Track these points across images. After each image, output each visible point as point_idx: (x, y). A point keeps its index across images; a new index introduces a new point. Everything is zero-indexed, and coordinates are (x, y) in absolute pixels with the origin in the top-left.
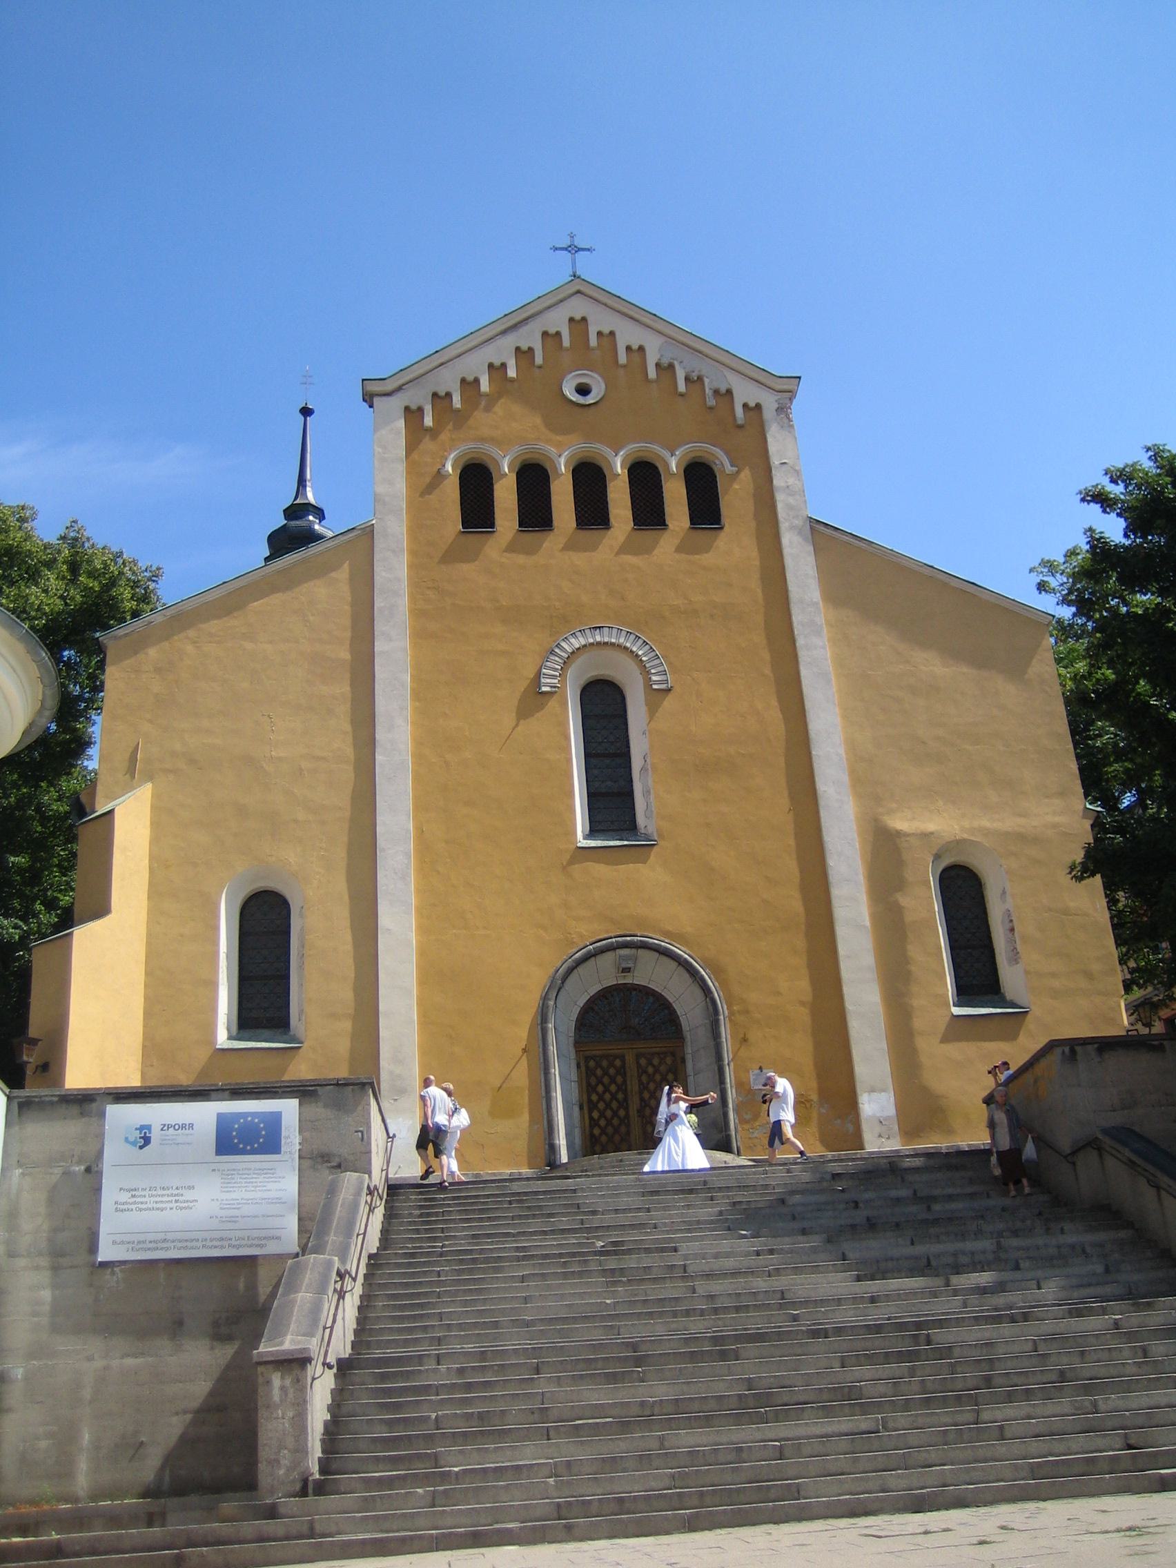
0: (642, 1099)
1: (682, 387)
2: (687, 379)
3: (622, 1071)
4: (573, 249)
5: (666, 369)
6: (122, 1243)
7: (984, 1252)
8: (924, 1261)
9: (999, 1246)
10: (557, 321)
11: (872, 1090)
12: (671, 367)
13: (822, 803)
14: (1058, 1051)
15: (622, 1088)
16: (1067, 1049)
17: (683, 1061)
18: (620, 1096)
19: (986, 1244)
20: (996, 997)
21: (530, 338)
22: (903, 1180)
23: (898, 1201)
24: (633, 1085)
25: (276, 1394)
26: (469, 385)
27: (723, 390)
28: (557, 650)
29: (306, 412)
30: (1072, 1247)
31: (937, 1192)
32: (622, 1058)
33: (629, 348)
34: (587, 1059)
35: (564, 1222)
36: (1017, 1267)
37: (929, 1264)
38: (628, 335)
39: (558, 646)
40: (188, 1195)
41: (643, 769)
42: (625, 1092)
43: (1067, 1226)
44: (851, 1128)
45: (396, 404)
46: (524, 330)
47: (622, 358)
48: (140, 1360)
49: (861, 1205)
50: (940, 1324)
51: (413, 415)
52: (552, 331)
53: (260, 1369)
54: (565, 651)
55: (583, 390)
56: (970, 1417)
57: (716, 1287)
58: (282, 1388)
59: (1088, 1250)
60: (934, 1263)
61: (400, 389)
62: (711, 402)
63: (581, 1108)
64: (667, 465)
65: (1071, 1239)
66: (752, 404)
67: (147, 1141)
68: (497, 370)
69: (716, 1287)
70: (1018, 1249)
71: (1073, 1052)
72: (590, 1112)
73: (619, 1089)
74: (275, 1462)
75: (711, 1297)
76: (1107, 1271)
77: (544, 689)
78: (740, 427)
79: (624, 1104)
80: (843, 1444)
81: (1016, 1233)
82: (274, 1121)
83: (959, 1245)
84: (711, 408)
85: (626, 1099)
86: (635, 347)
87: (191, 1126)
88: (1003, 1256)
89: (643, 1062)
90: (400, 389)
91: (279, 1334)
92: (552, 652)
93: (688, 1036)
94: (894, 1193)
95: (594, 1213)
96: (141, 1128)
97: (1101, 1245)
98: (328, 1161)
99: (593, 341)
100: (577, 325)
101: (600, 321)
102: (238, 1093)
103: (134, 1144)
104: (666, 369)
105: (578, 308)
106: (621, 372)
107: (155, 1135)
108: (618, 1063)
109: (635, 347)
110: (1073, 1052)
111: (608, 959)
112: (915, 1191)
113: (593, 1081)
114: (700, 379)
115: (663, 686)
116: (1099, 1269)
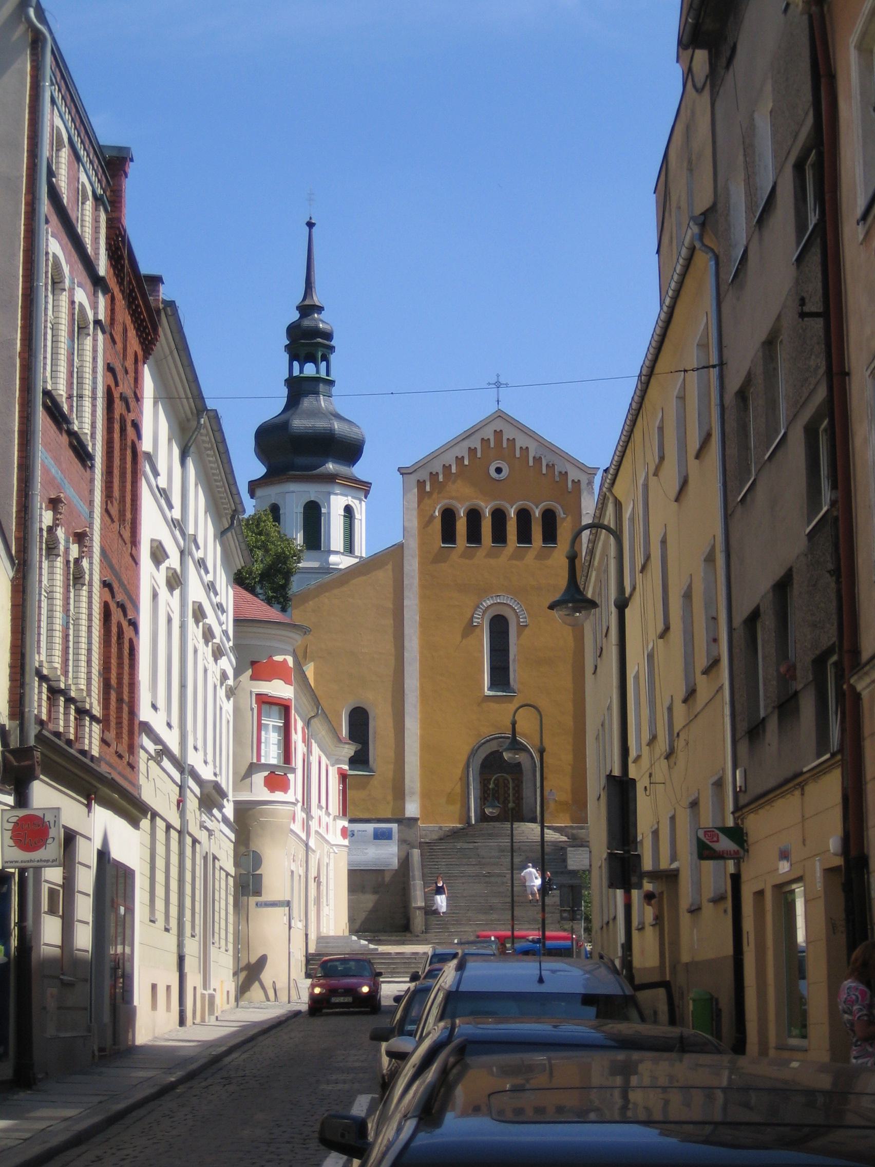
1: (544, 471)
2: (547, 465)
4: (498, 385)
5: (538, 460)
10: (488, 433)
12: (540, 458)
17: (522, 782)
21: (475, 443)
26: (447, 468)
29: (310, 225)
34: (484, 780)
38: (522, 441)
39: (482, 604)
40: (366, 851)
41: (514, 660)
45: (413, 479)
46: (473, 437)
47: (518, 455)
51: (421, 484)
54: (484, 606)
55: (499, 470)
62: (557, 479)
63: (481, 799)
67: (353, 835)
68: (460, 460)
77: (475, 624)
82: (390, 830)
84: (557, 482)
86: (524, 448)
92: (478, 607)
93: (524, 772)
101: (509, 433)
104: (538, 460)
105: (498, 425)
107: (356, 833)
109: (524, 448)
111: (495, 742)
114: (553, 465)
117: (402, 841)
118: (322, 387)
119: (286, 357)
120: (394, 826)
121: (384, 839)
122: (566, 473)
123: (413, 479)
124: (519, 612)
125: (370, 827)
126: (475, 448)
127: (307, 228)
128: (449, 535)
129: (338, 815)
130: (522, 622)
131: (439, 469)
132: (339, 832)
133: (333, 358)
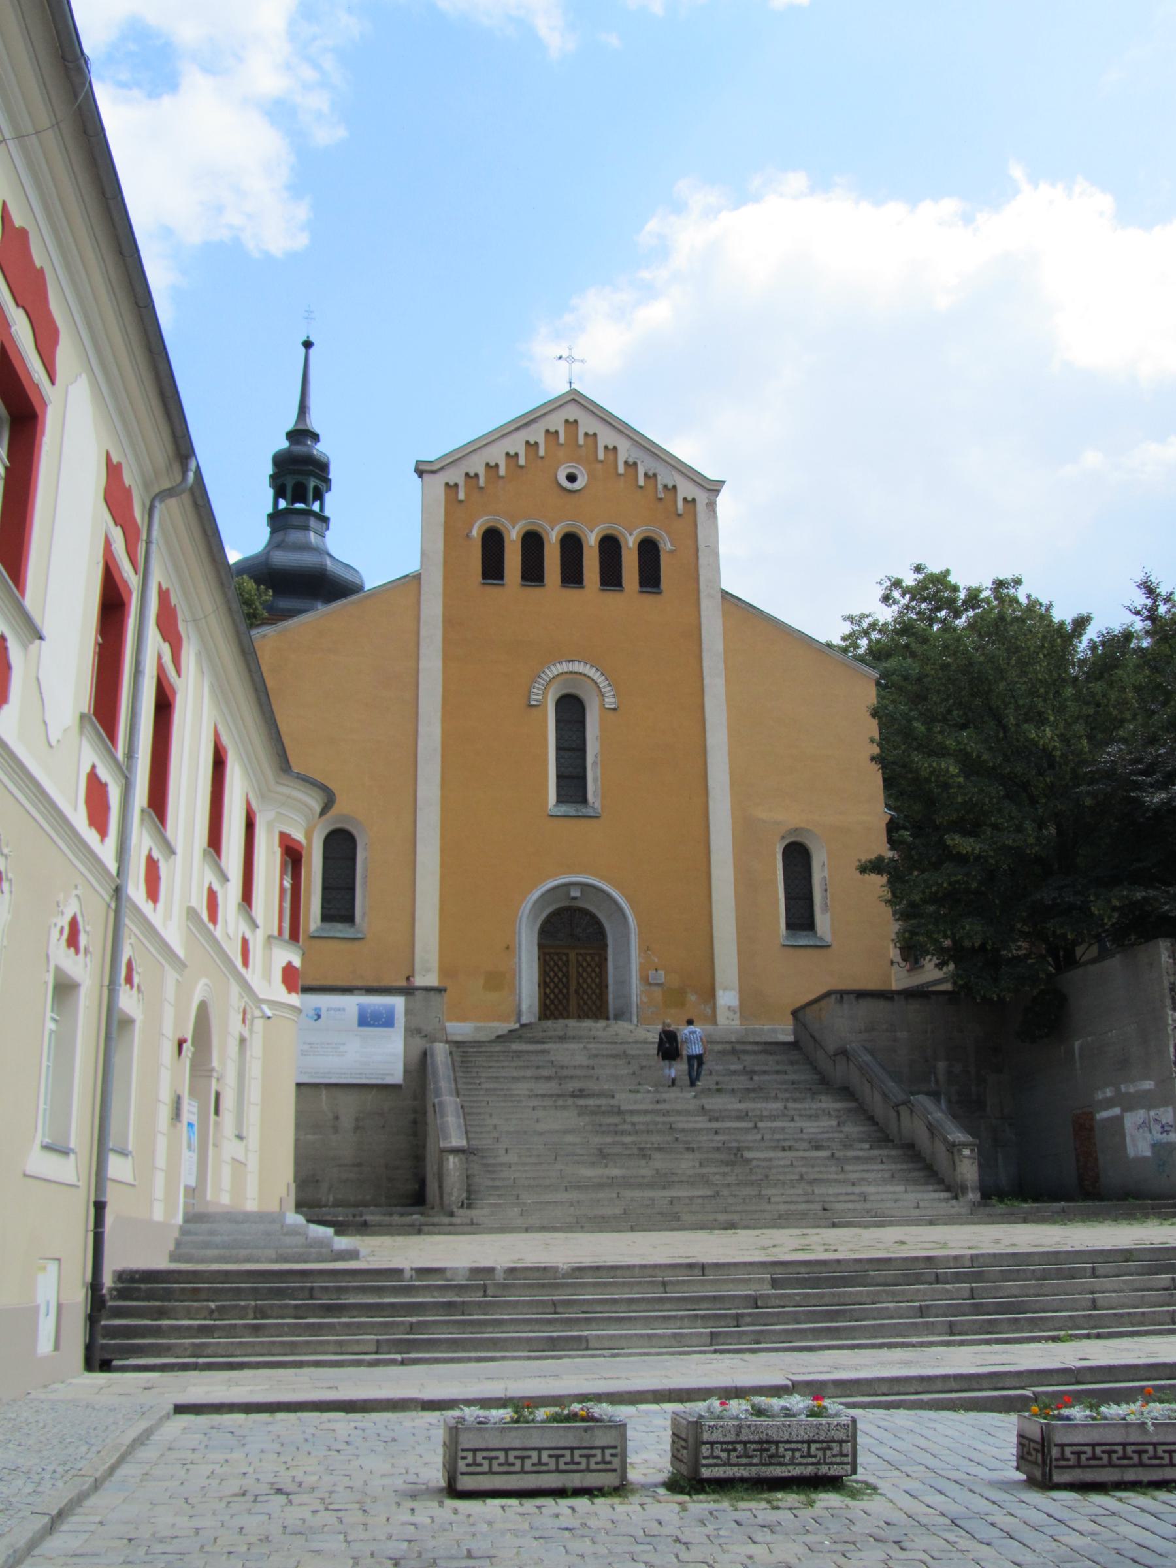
0: (578, 983)
1: (641, 482)
2: (646, 475)
3: (567, 964)
5: (632, 466)
6: (305, 1073)
7: (777, 1109)
8: (744, 1113)
9: (785, 1108)
10: (556, 423)
11: (725, 989)
12: (635, 464)
13: (711, 795)
14: (833, 997)
15: (566, 975)
16: (838, 996)
18: (564, 980)
19: (779, 1105)
20: (811, 933)
21: (536, 434)
22: (739, 1059)
23: (734, 1073)
24: (573, 972)
25: (451, 1165)
26: (492, 468)
27: (670, 486)
28: (542, 675)
29: (308, 345)
30: (823, 1110)
31: (757, 1068)
32: (567, 955)
33: (606, 447)
35: (545, 1073)
36: (793, 1120)
37: (747, 1115)
38: (607, 437)
40: (342, 1048)
41: (595, 763)
42: (567, 978)
43: (823, 1098)
44: (709, 1011)
45: (438, 481)
46: (534, 426)
47: (601, 455)
48: (316, 1137)
49: (714, 1073)
50: (749, 1149)
51: (451, 488)
52: (552, 430)
53: (444, 1154)
54: (548, 676)
55: (572, 478)
56: (756, 1193)
57: (636, 1119)
58: (454, 1163)
59: (832, 1112)
60: (750, 1114)
61: (442, 468)
62: (661, 495)
64: (627, 542)
65: (824, 1105)
66: (689, 499)
67: (319, 1016)
68: (511, 457)
69: (636, 1119)
70: (795, 1109)
71: (842, 997)
72: (544, 989)
73: (564, 975)
74: (451, 1194)
75: (633, 1124)
76: (839, 1125)
77: (533, 703)
78: (679, 515)
79: (566, 986)
80: (700, 1201)
81: (795, 1100)
83: (764, 1105)
84: (661, 499)
85: (568, 982)
86: (611, 447)
87: (344, 1010)
88: (786, 1112)
89: (580, 958)
90: (442, 468)
91: (447, 1137)
92: (539, 677)
94: (733, 1067)
95: (562, 1067)
96: (316, 1009)
97: (838, 1111)
98: (420, 1033)
99: (581, 441)
100: (572, 424)
101: (587, 425)
102: (370, 990)
103: (312, 1018)
104: (632, 466)
105: (572, 412)
106: (599, 466)
107: (324, 1014)
108: (564, 958)
109: (611, 447)
110: (842, 997)
112: (745, 1067)
113: (548, 969)
114: (655, 475)
115: (613, 706)
116: (834, 1123)
117: (412, 1031)
118: (313, 522)
119: (270, 492)
120: (398, 1003)
121: (378, 1026)
122: (674, 487)
123: (438, 481)
124: (605, 687)
125: (351, 1004)
126: (536, 443)
127: (303, 350)
128: (493, 569)
129: (276, 933)
130: (611, 703)
131: (481, 471)
132: (277, 975)
133: (328, 497)
